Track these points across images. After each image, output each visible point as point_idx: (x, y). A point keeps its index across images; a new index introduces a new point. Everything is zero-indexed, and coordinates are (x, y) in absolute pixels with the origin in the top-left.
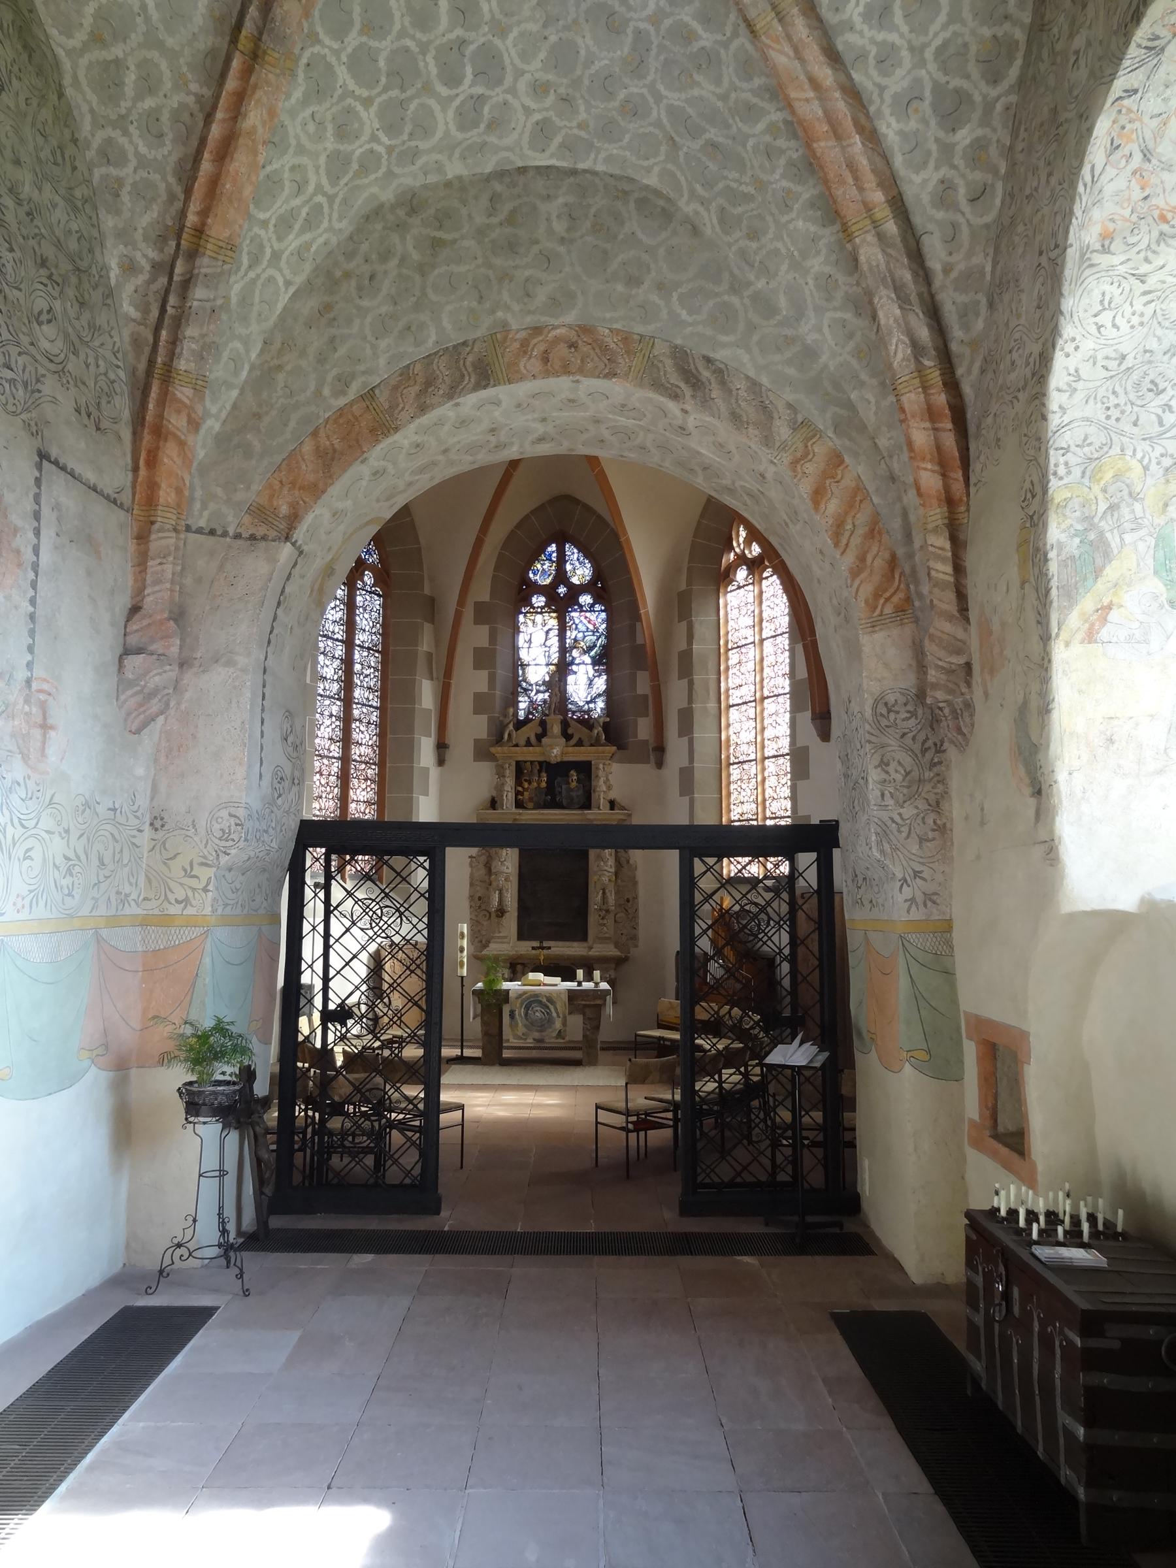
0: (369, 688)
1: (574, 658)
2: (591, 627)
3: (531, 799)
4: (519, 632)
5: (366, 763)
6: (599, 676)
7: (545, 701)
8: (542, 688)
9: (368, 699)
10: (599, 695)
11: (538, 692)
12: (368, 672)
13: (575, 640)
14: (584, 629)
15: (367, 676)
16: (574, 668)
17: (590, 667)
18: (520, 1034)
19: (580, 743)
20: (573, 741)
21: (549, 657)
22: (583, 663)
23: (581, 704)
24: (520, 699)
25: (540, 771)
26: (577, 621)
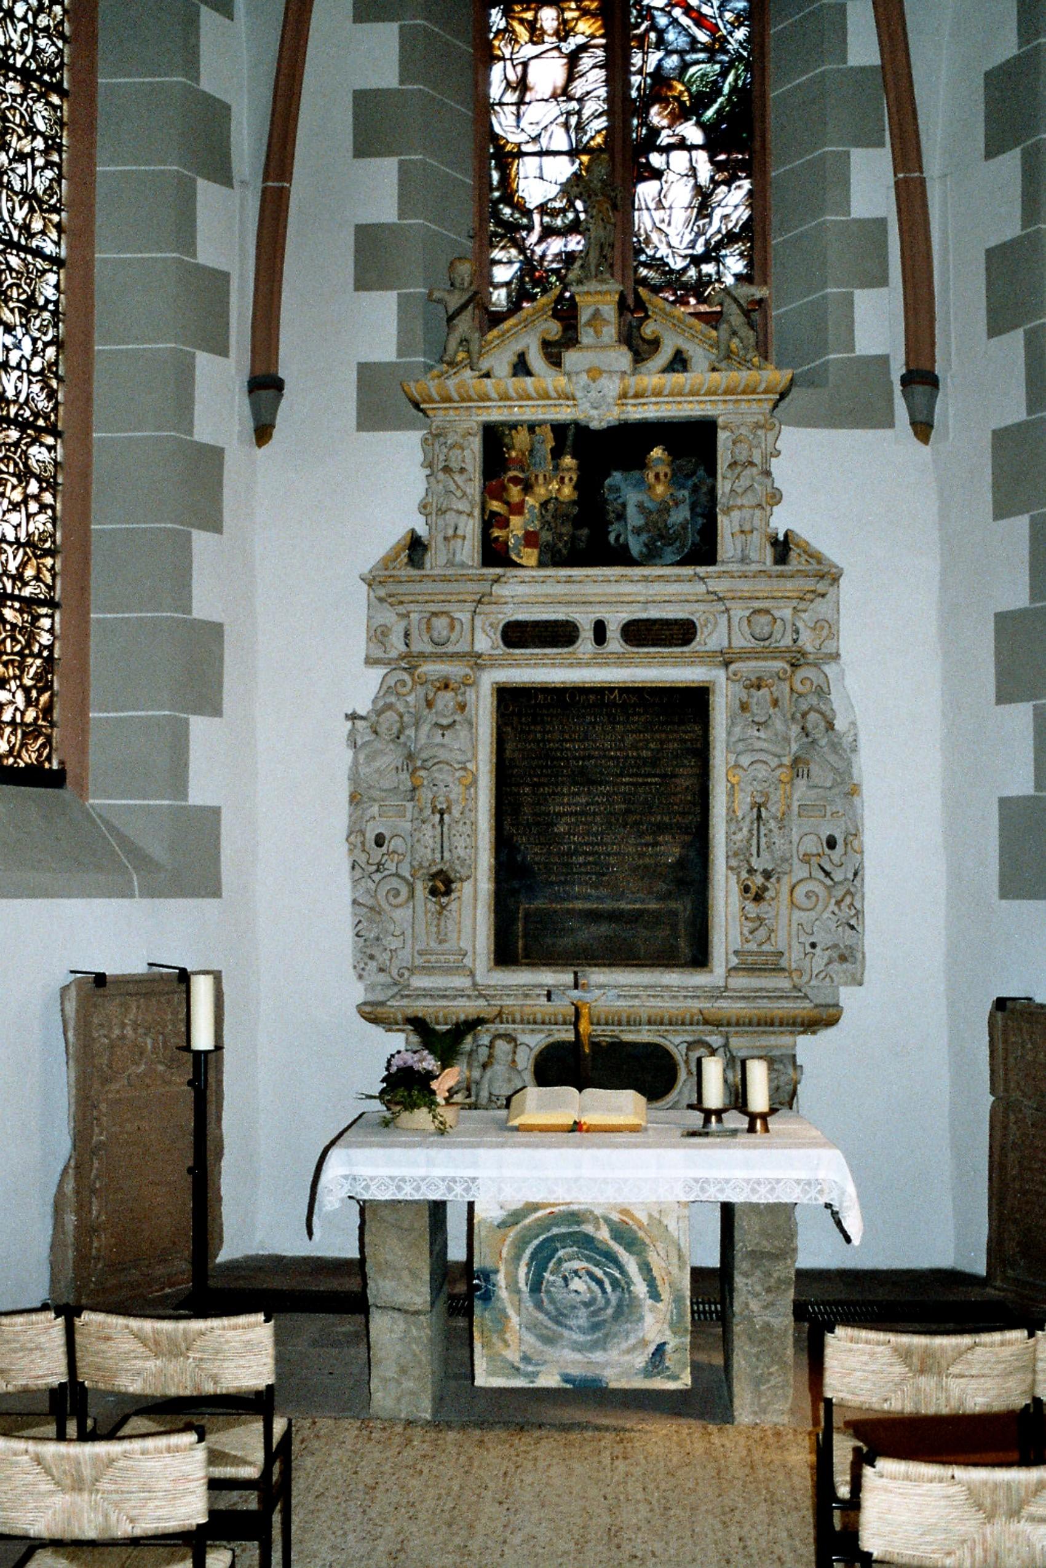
0: (29, 197)
1: (655, 132)
2: (703, 37)
3: (530, 539)
4: (490, 58)
5: (23, 426)
6: (728, 183)
7: (569, 258)
8: (559, 222)
9: (25, 228)
10: (731, 238)
11: (548, 232)
12: (26, 146)
13: (659, 76)
14: (682, 42)
15: (21, 157)
16: (656, 160)
17: (701, 158)
18: (512, 1355)
19: (679, 362)
20: (664, 356)
21: (580, 128)
22: (682, 145)
23: (678, 264)
24: (497, 254)
25: (557, 453)
26: (662, 21)
